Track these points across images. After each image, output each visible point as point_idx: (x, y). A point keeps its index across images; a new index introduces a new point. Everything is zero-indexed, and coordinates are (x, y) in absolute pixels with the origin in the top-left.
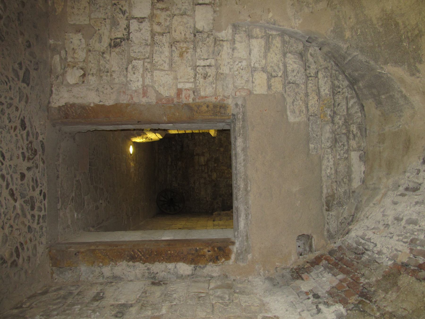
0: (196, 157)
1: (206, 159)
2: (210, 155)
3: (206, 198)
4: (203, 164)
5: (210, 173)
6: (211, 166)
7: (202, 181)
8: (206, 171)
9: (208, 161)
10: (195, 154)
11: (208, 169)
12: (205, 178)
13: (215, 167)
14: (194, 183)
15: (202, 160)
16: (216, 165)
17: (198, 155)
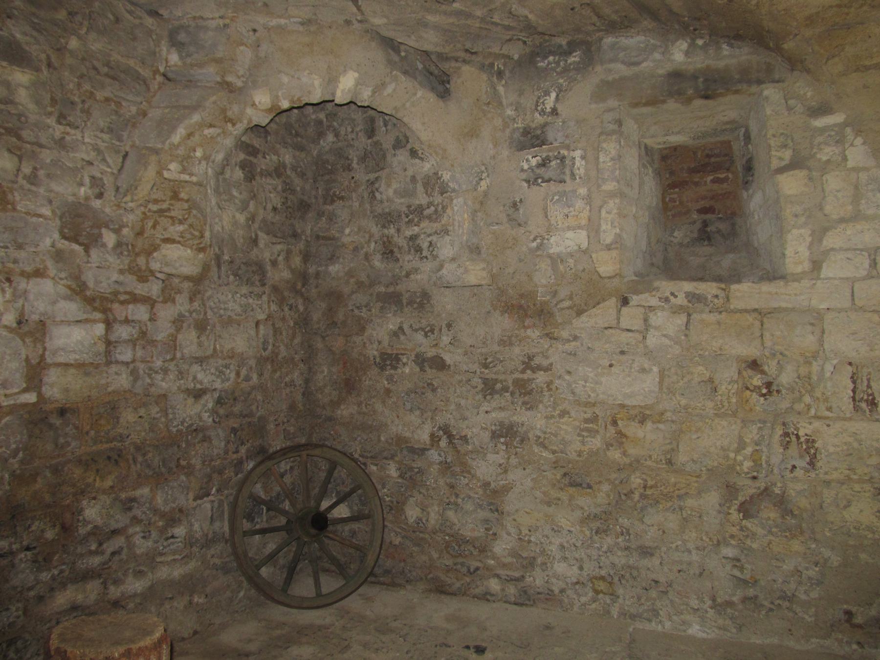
0: (57, 386)
1: (72, 308)
2: (39, 273)
3: (257, 324)
4: (100, 329)
5: (154, 289)
6: (115, 276)
7: (189, 340)
8: (141, 312)
9: (79, 290)
10: (31, 398)
11: (135, 299)
12: (178, 322)
13: (119, 244)
14: (198, 394)
15: (74, 338)
16: (109, 238)
17: (35, 374)
